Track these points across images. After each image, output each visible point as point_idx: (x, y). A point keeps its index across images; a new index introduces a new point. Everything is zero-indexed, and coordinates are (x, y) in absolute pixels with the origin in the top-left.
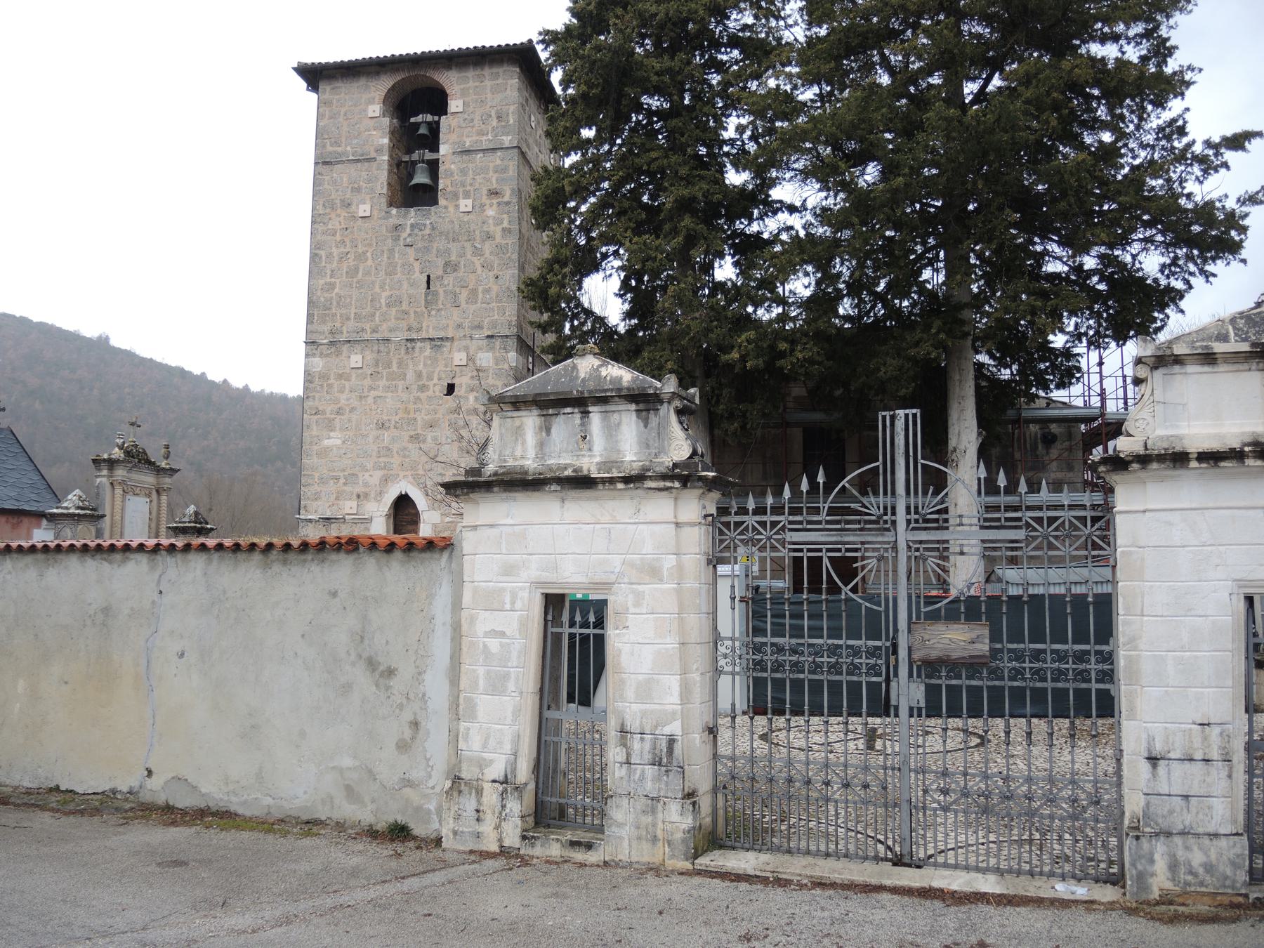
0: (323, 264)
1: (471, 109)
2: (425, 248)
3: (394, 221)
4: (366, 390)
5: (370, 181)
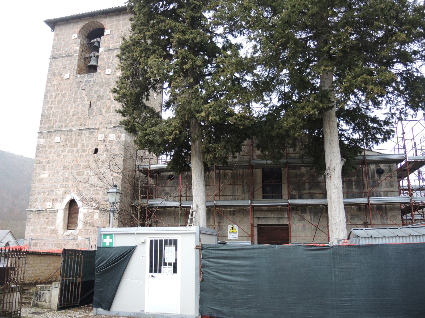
0: (48, 99)
1: (113, 33)
2: (90, 90)
3: (78, 80)
4: (60, 152)
5: (70, 64)
